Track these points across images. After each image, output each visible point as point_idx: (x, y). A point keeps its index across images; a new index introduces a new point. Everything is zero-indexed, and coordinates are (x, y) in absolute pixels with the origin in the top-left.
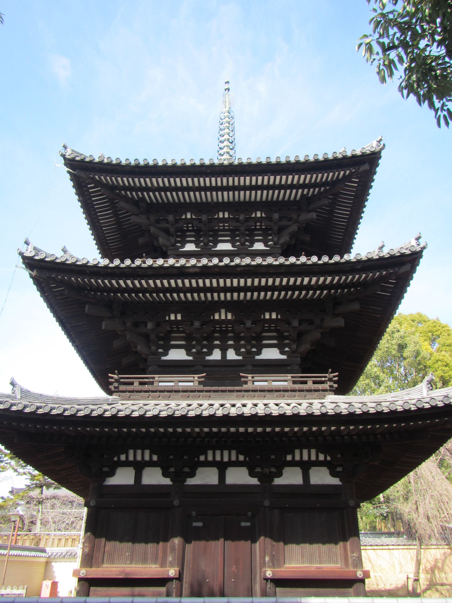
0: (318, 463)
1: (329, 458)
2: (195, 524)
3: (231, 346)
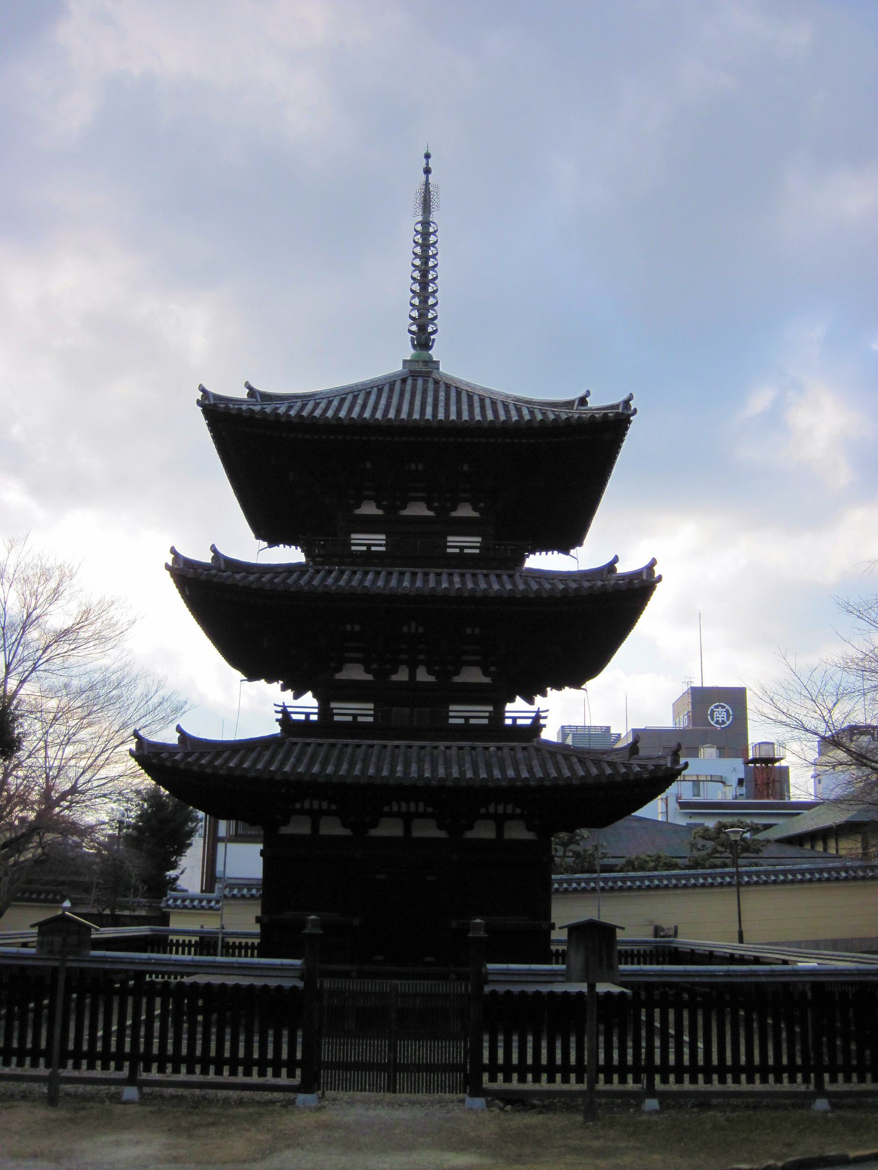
0: (513, 817)
1: (526, 812)
2: (378, 877)
3: (421, 663)
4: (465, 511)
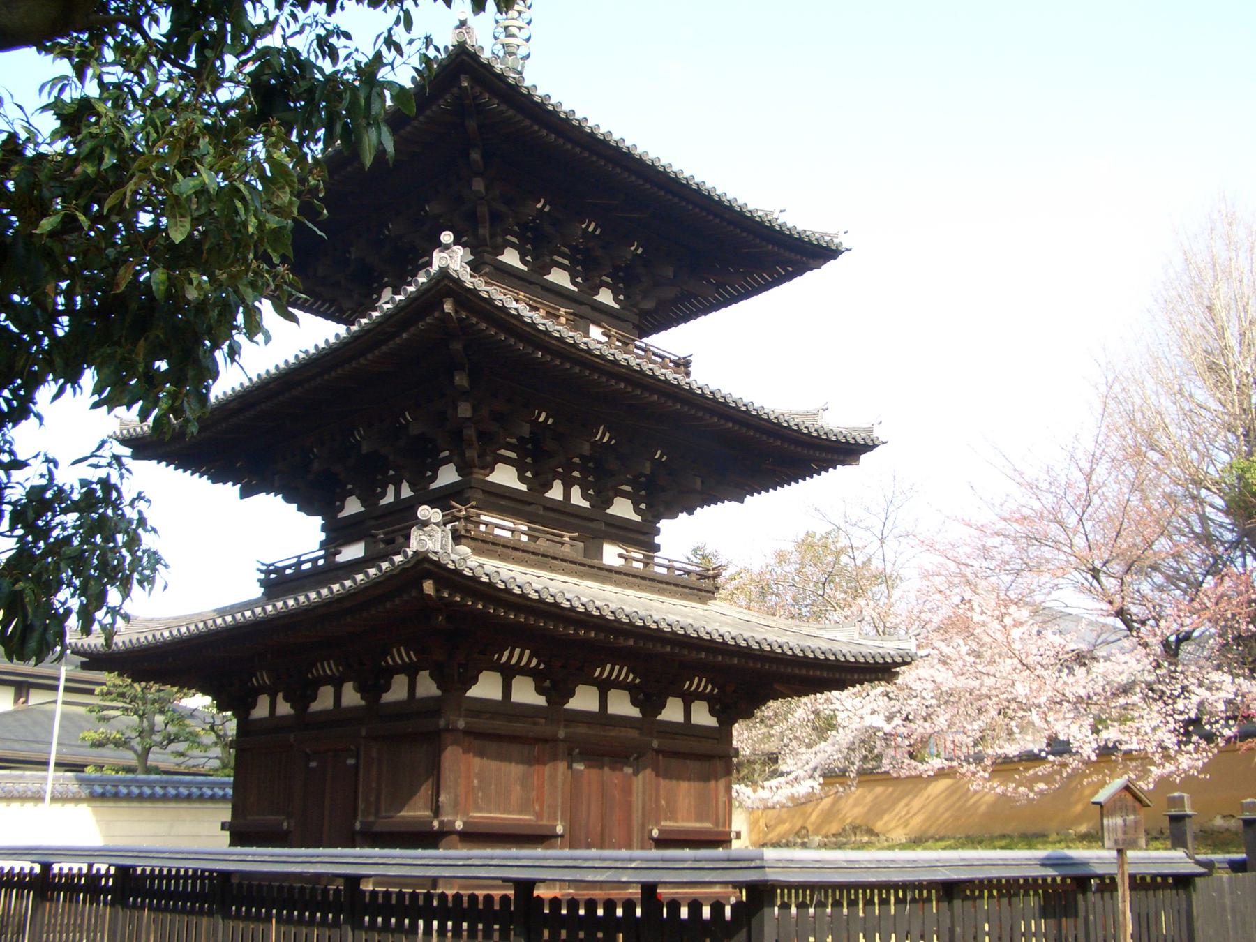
4: (605, 297)
